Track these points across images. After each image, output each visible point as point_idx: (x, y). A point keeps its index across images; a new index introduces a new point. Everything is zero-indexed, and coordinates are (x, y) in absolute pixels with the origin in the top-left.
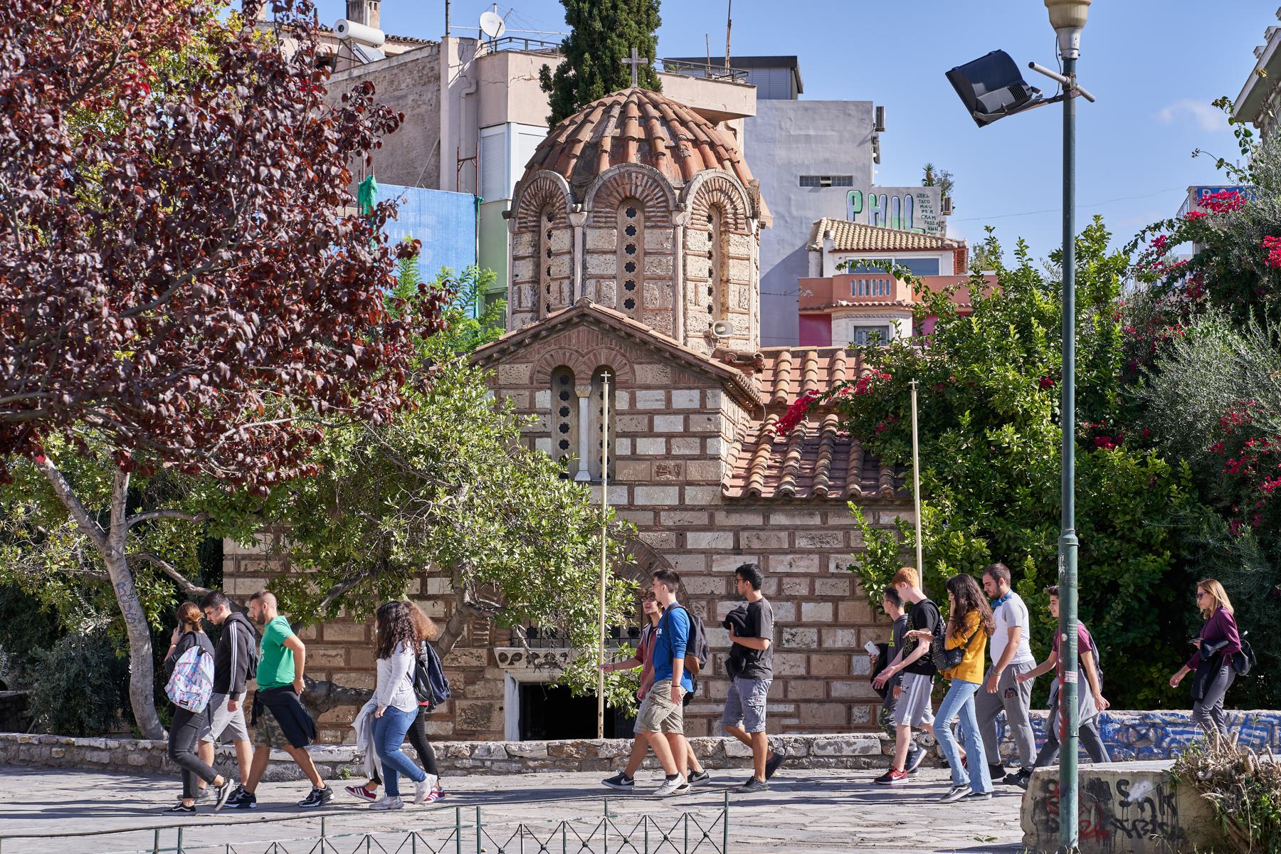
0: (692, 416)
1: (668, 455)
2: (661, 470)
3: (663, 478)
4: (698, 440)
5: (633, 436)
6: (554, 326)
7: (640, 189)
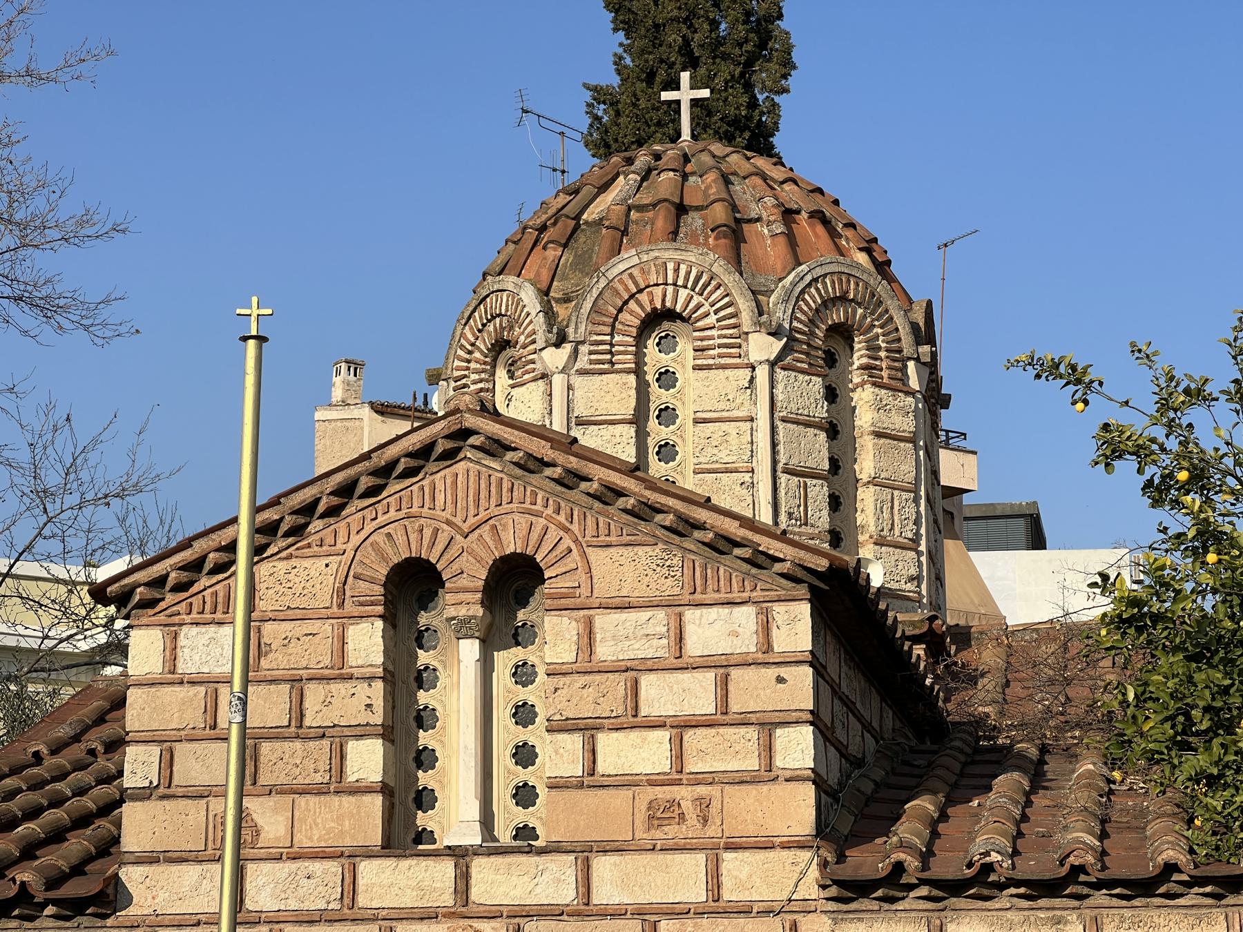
0: (735, 673)
1: (678, 775)
2: (661, 814)
3: (672, 831)
4: (752, 733)
5: (588, 728)
6: (393, 463)
7: (683, 294)
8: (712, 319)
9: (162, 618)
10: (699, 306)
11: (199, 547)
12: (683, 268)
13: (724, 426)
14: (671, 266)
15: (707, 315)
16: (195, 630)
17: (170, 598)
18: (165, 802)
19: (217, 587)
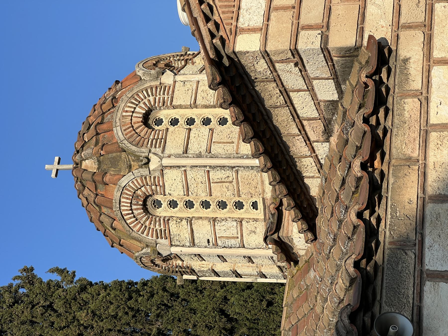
8: (151, 99)
9: (231, 38)
10: (145, 103)
11: (197, 14)
12: (127, 109)
13: (199, 91)
14: (124, 114)
15: (149, 101)
16: (241, 19)
17: (222, 33)
18: (331, 28)
19: (220, 12)
